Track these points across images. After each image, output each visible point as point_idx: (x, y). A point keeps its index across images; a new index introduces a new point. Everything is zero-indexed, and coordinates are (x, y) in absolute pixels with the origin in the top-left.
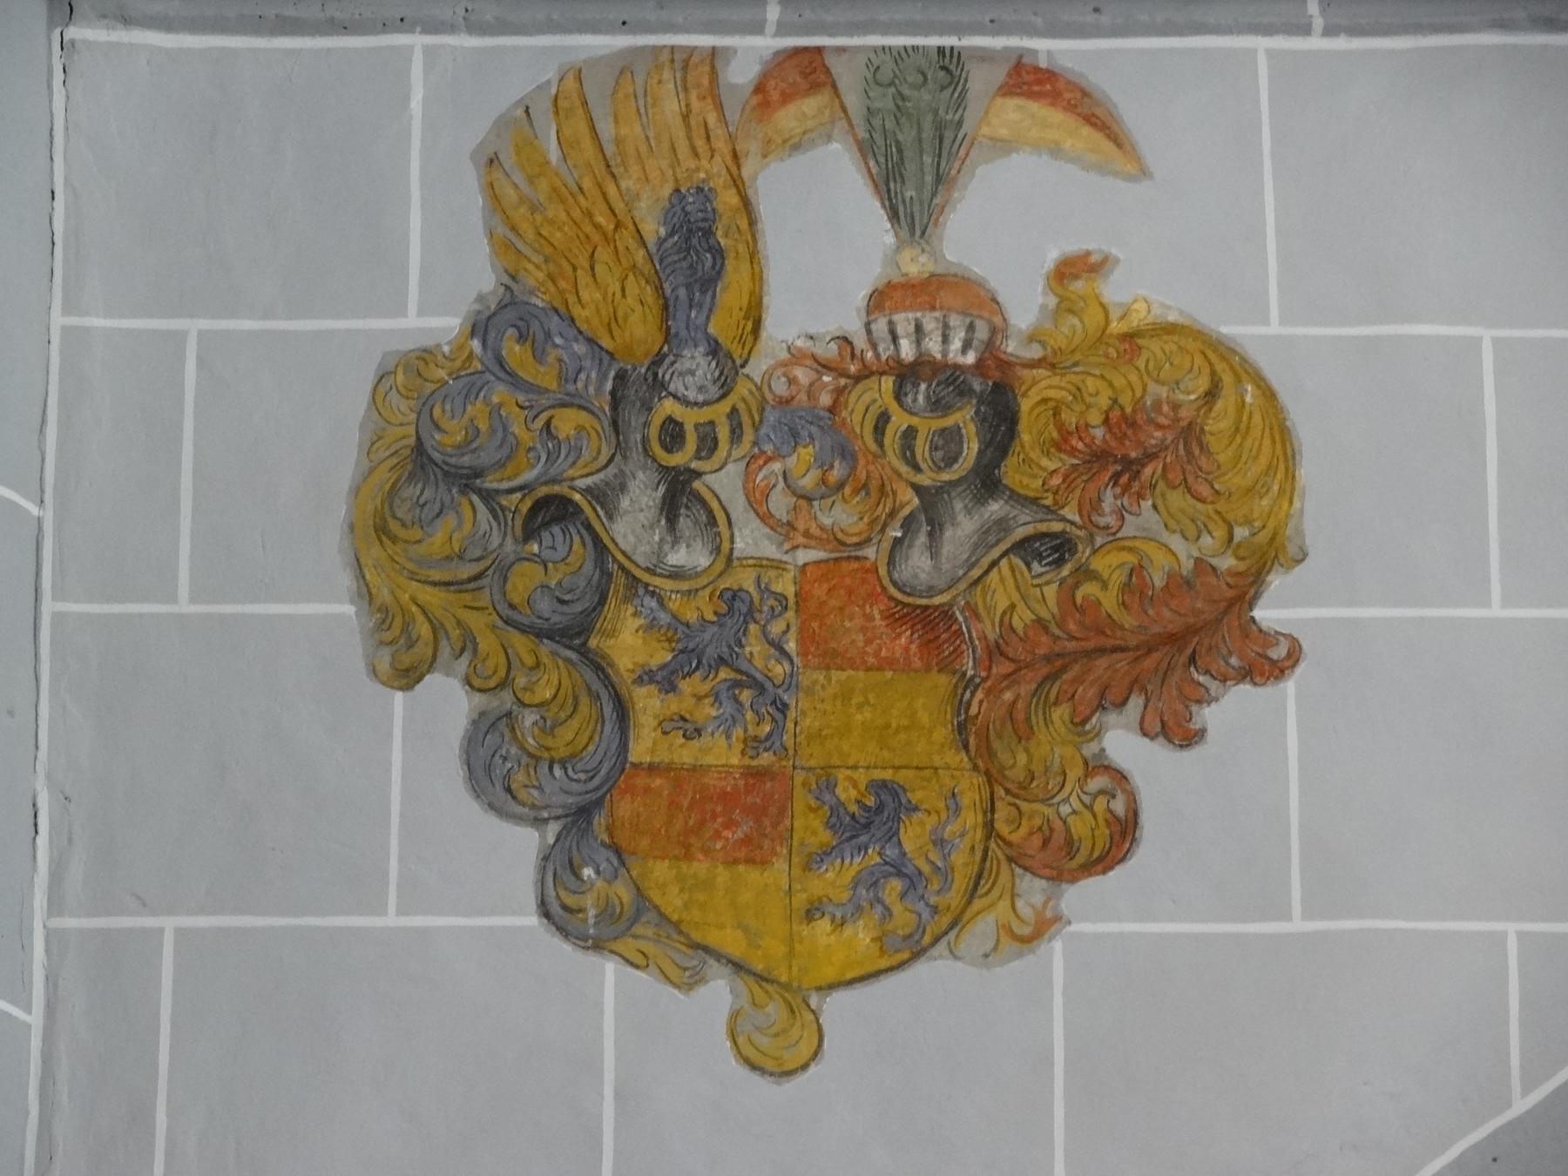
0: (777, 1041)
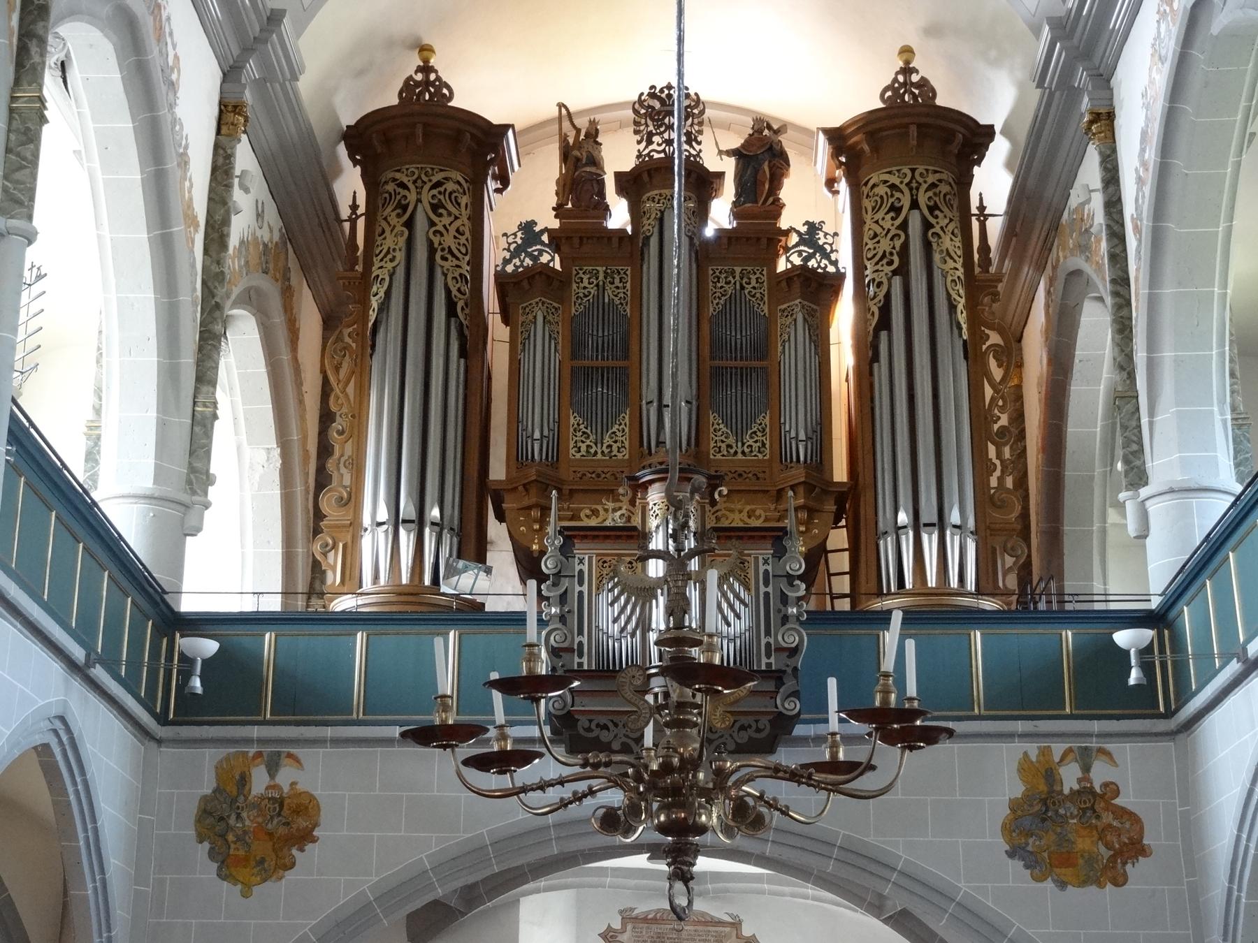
0: (246, 894)
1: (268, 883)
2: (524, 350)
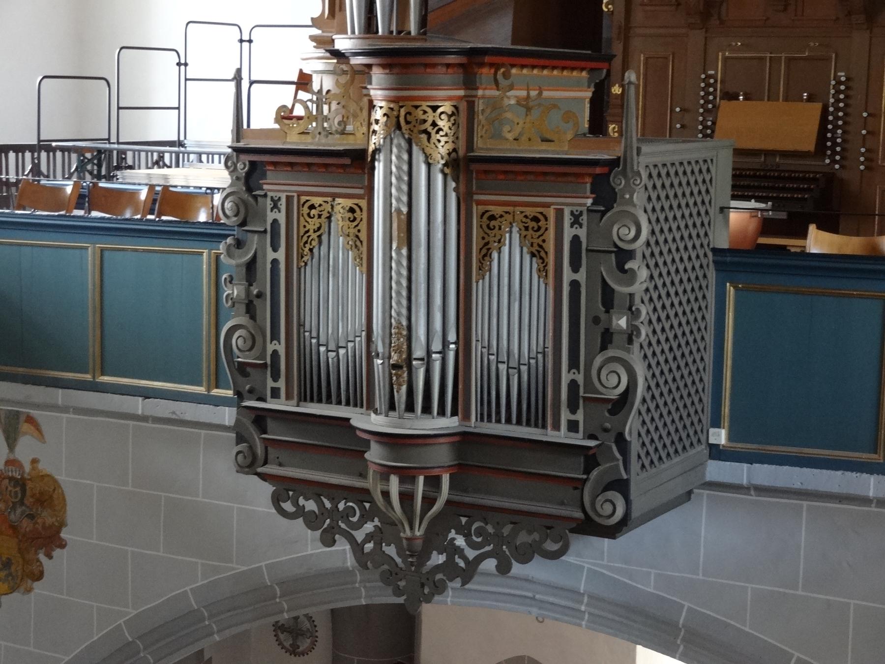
1: (15, 594)
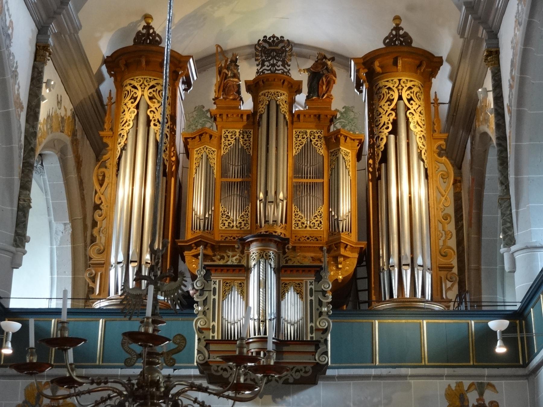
2: (196, 173)
